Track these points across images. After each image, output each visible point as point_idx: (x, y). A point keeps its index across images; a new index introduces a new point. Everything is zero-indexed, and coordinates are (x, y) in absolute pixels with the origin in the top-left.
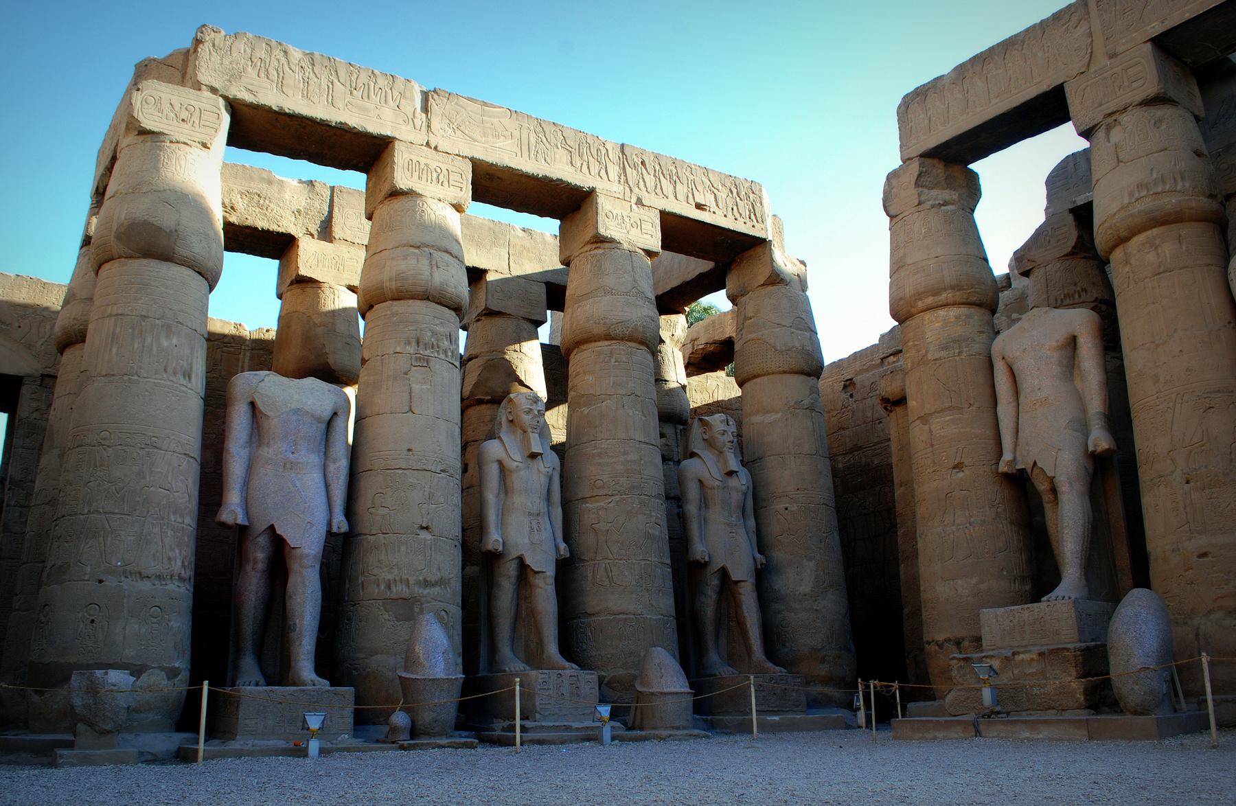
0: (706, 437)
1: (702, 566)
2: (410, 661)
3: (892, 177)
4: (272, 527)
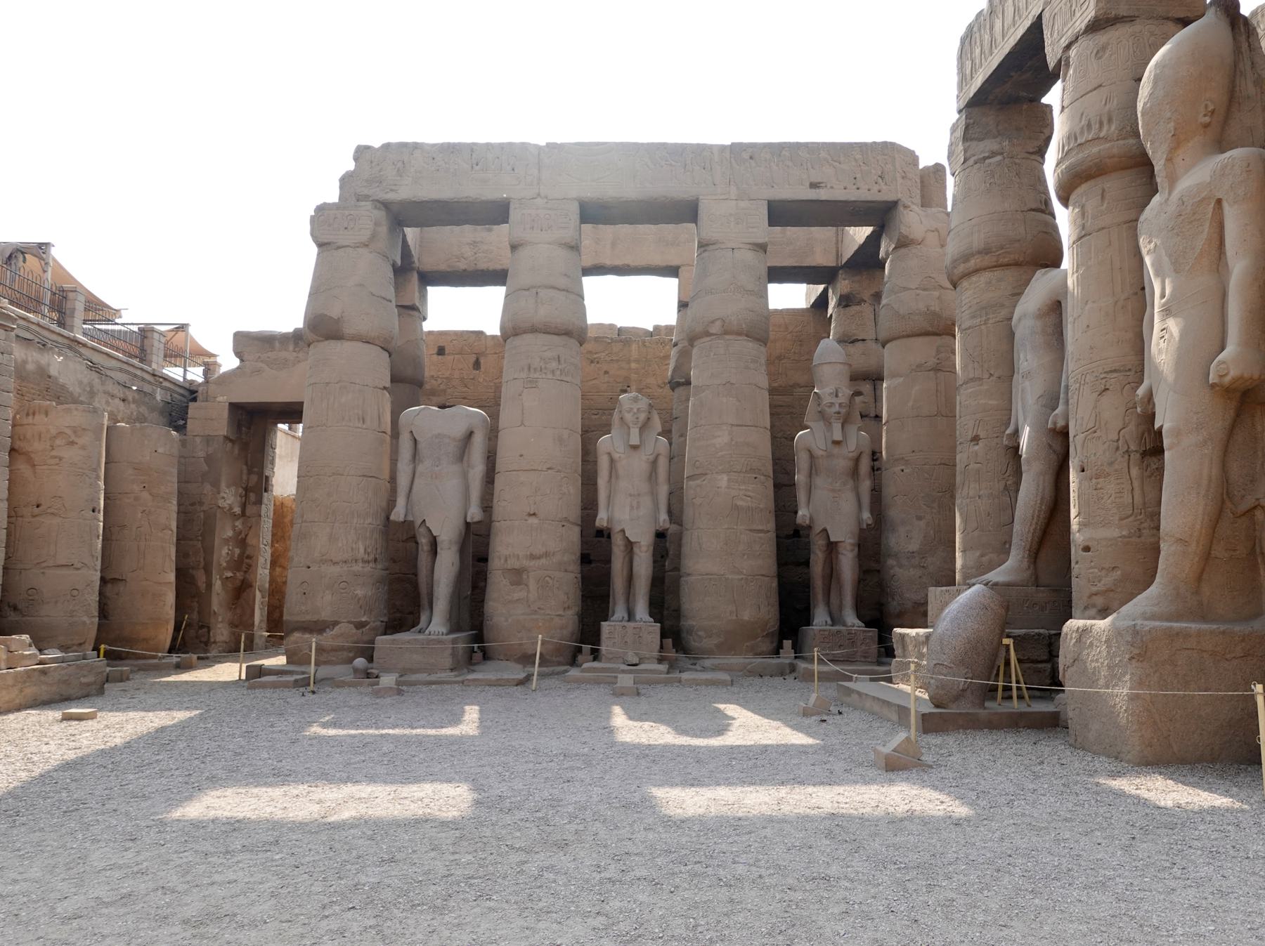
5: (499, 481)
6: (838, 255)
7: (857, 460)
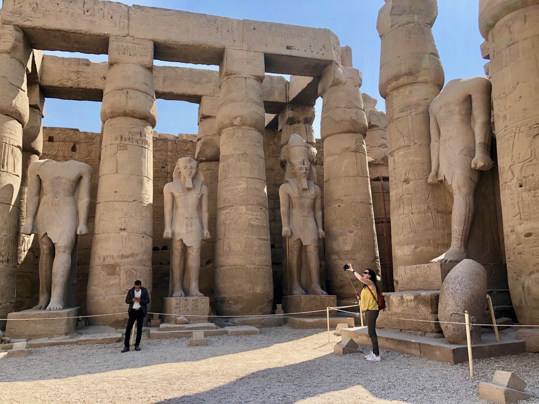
0: (294, 171)
3: (381, 11)
5: (100, 210)
6: (287, 97)
7: (315, 200)
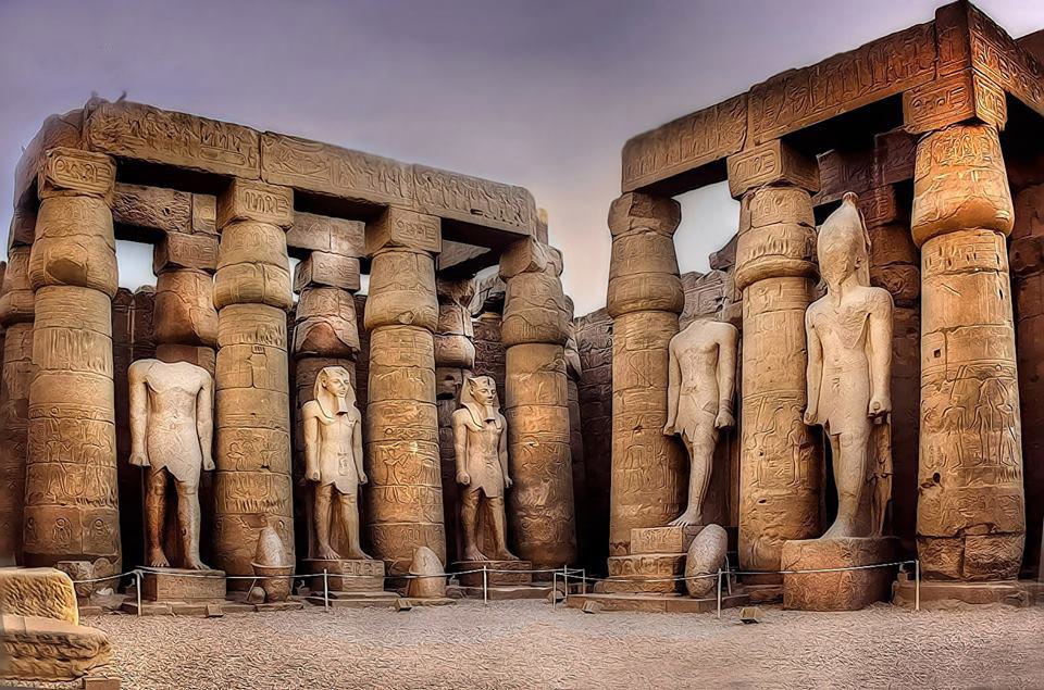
1: (464, 487)
2: (259, 556)
4: (165, 467)
